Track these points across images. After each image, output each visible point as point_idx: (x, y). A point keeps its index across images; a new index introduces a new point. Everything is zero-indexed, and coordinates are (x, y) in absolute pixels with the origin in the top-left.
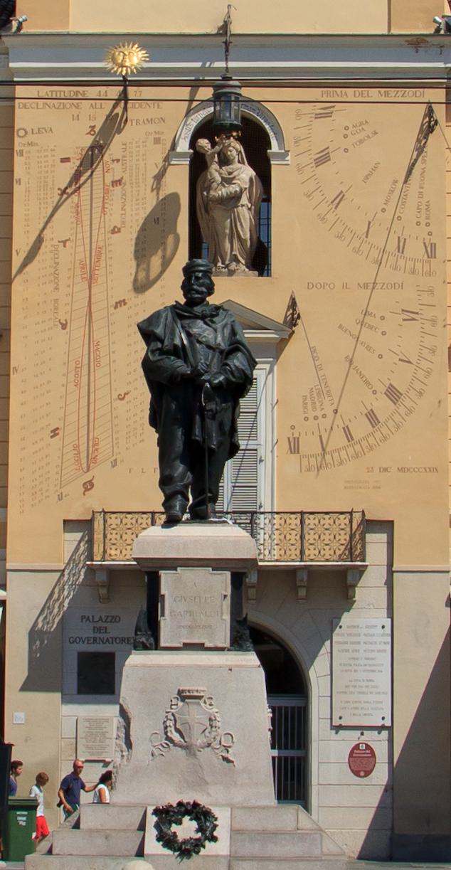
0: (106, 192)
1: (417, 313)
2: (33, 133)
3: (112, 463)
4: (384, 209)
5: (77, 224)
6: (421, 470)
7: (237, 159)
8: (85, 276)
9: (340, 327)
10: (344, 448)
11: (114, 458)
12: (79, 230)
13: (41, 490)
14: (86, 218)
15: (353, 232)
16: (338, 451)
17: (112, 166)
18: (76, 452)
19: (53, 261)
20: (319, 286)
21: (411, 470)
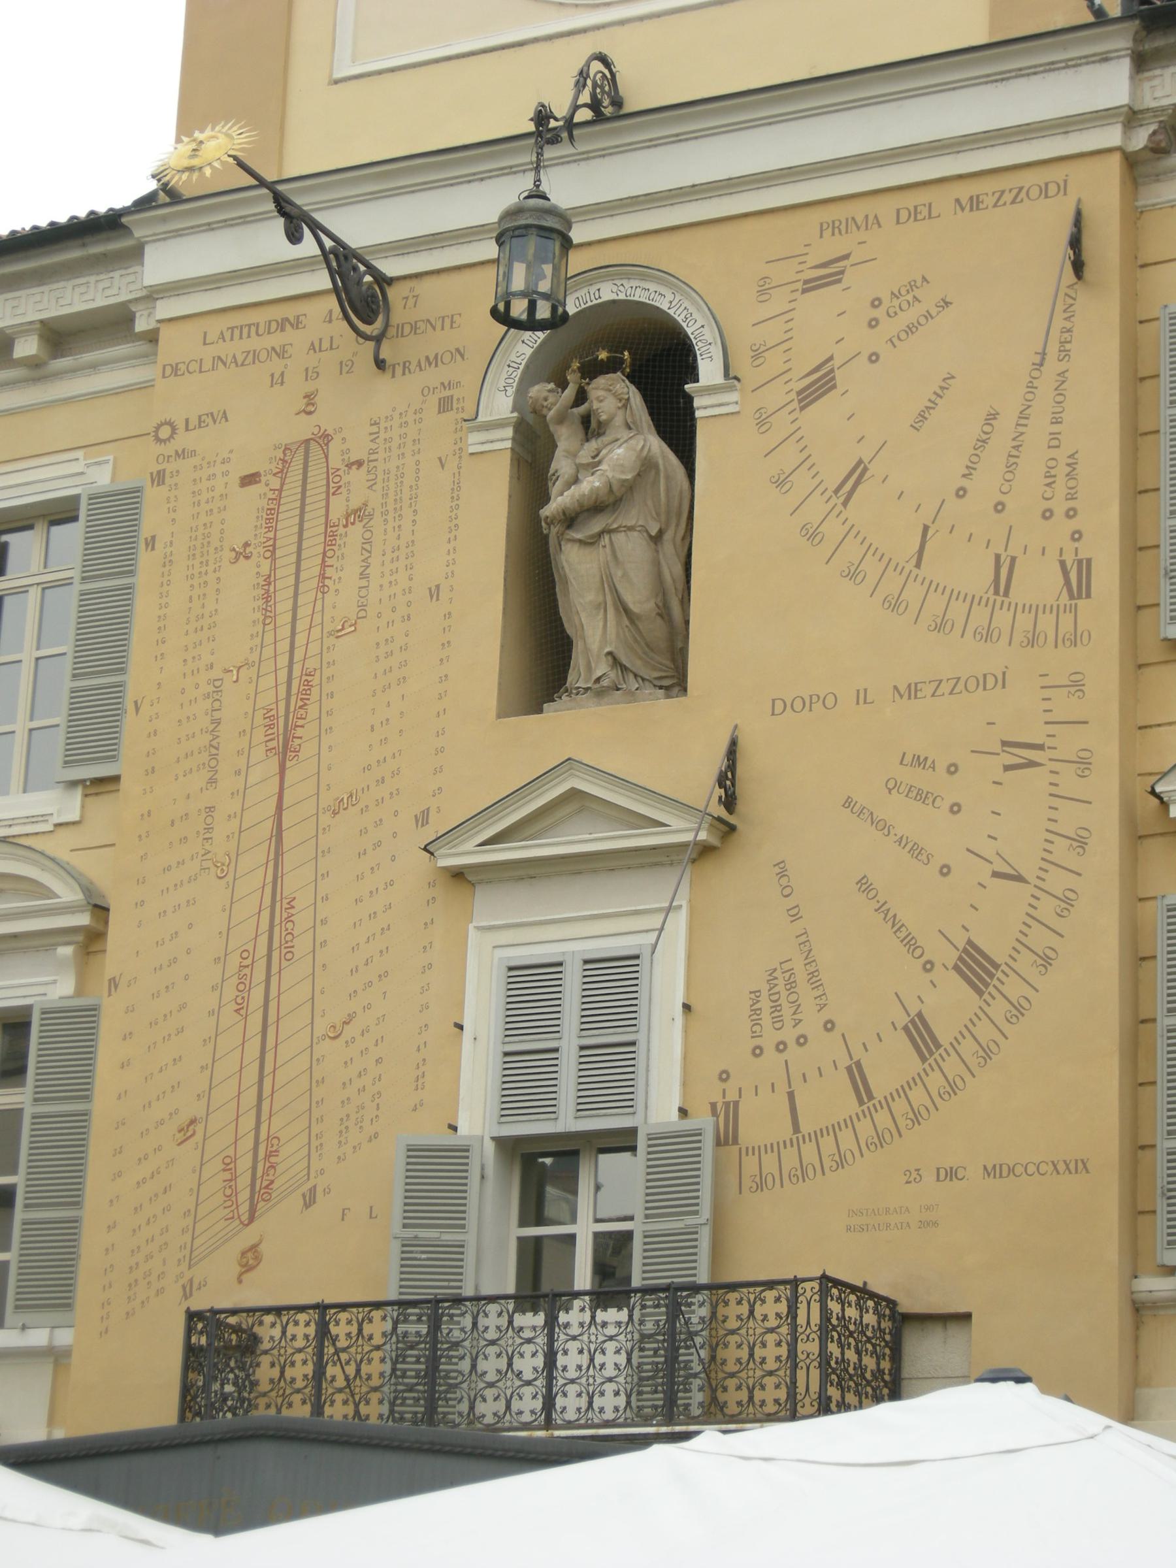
0: (330, 537)
1: (1040, 747)
2: (187, 429)
3: (304, 1196)
4: (962, 488)
5: (265, 625)
6: (1043, 1168)
7: (619, 420)
8: (273, 744)
9: (848, 803)
10: (850, 1123)
11: (309, 1185)
12: (269, 638)
13: (148, 1274)
14: (284, 607)
15: (886, 559)
16: (834, 1130)
17: (346, 479)
18: (227, 1176)
19: (209, 718)
20: (798, 705)
21: (1019, 1170)
